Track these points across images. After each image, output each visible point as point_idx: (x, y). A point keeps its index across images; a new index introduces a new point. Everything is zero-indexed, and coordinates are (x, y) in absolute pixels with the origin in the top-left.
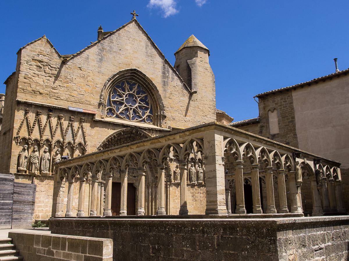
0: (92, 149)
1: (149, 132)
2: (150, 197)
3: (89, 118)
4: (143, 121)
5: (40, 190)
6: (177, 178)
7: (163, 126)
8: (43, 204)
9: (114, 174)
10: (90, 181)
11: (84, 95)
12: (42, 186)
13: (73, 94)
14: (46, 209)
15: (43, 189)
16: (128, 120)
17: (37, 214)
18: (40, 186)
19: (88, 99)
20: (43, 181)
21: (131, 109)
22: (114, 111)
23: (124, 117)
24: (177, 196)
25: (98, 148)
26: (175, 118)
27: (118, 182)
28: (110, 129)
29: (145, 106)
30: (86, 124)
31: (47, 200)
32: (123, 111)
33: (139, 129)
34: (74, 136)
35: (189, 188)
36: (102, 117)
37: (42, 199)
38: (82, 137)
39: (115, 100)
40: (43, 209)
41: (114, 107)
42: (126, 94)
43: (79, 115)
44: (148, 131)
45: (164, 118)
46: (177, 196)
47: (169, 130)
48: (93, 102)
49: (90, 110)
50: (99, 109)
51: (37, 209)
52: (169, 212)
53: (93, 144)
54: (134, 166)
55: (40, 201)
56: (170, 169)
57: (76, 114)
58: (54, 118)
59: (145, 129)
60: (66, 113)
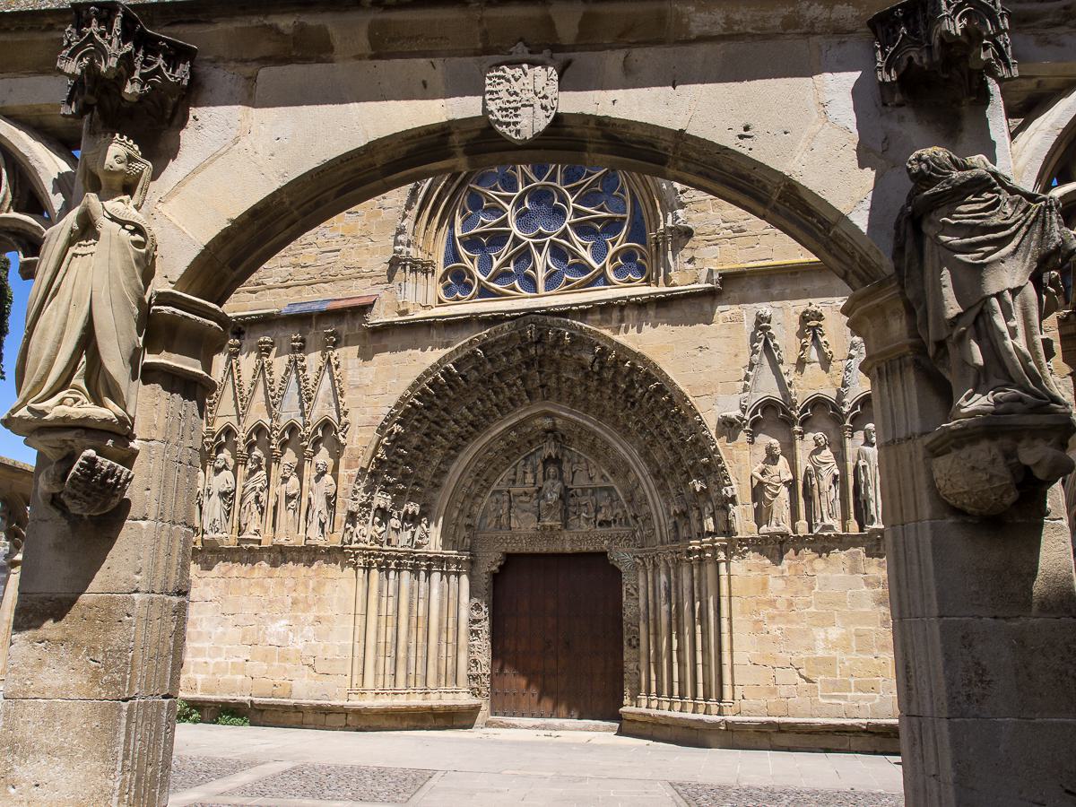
0: (362, 435)
1: (604, 322)
2: (664, 608)
3: (354, 325)
4: (601, 279)
5: (201, 596)
6: (770, 510)
7: (675, 280)
8: (207, 645)
9: (513, 520)
10: (356, 557)
11: (339, 251)
12: (207, 584)
13: (301, 261)
14: (216, 660)
15: (210, 593)
16: (529, 294)
17: (191, 675)
18: (201, 582)
19: (353, 259)
20: (209, 568)
21: (540, 247)
22: (472, 277)
23: (514, 289)
24: (775, 601)
25: (382, 427)
26: (741, 223)
27: (530, 550)
28: (430, 347)
29: (605, 218)
30: (344, 348)
31: (220, 629)
32: (506, 263)
33: (549, 319)
34: (306, 398)
35: (854, 557)
36: (402, 309)
37: (205, 627)
38: (331, 400)
39: (473, 231)
40: (208, 659)
41: (472, 260)
42: (517, 194)
43: (322, 325)
44: (598, 317)
45: (683, 239)
46: (775, 601)
47: (709, 285)
48: (368, 264)
49: (358, 291)
50: (391, 285)
51: (191, 659)
52: (733, 685)
53: (368, 417)
54: (603, 476)
55: (200, 634)
56: (723, 469)
57: (314, 323)
58: (248, 356)
59: (583, 312)
60: (284, 328)
